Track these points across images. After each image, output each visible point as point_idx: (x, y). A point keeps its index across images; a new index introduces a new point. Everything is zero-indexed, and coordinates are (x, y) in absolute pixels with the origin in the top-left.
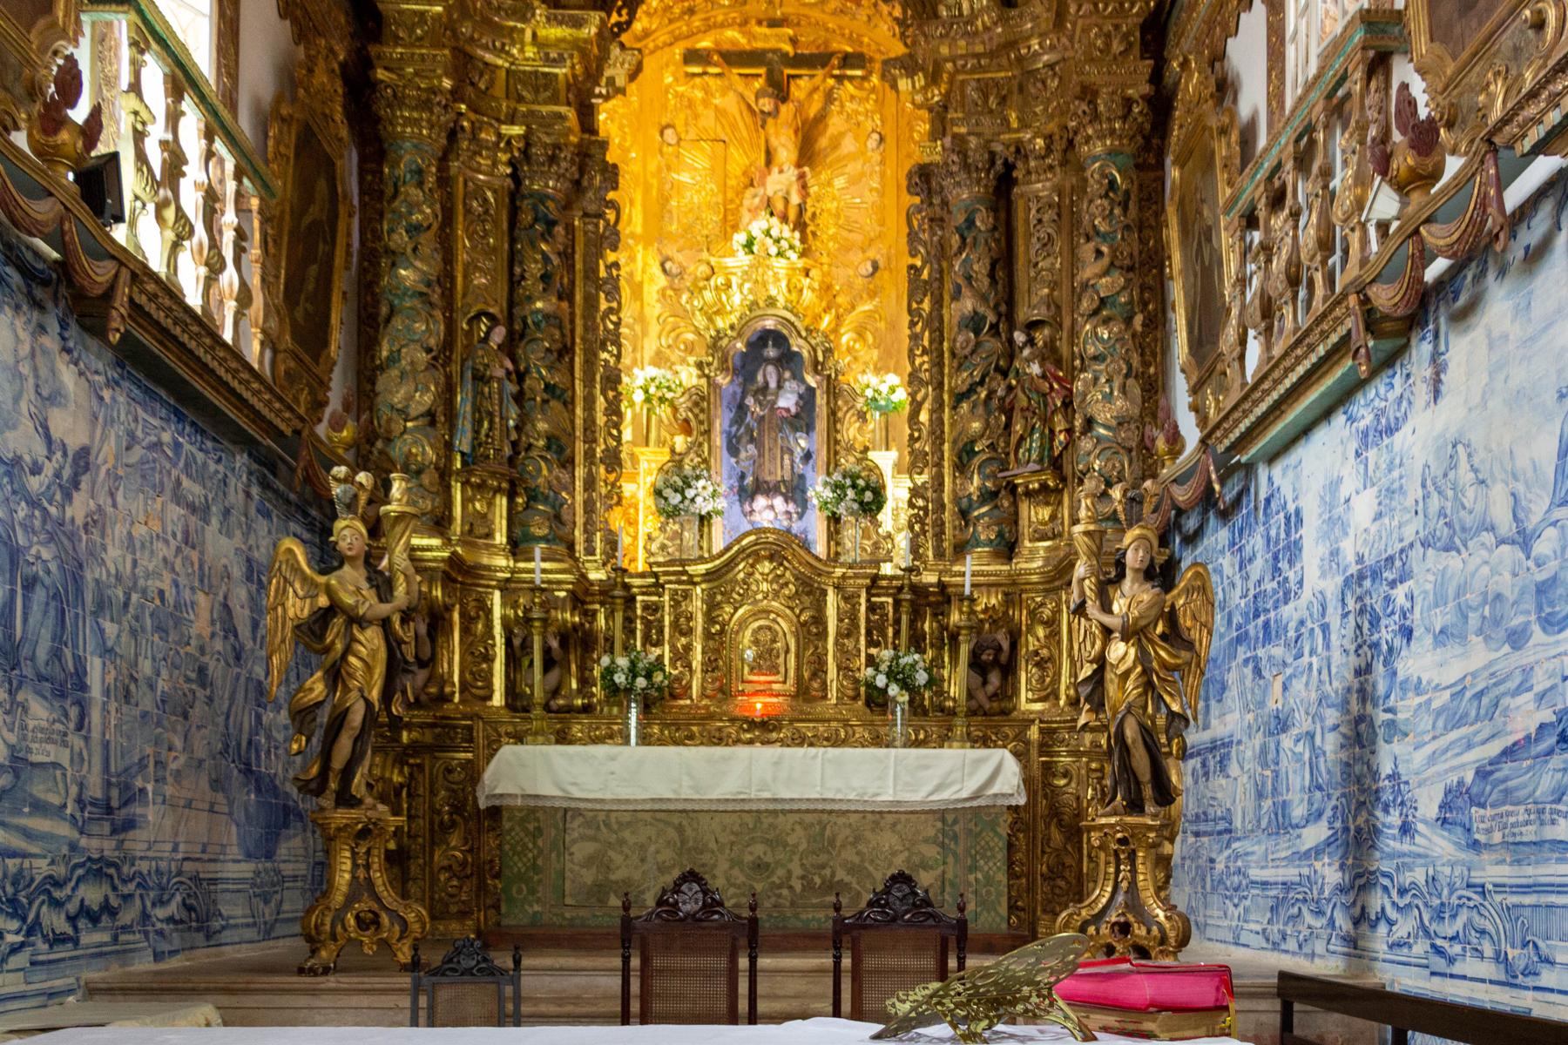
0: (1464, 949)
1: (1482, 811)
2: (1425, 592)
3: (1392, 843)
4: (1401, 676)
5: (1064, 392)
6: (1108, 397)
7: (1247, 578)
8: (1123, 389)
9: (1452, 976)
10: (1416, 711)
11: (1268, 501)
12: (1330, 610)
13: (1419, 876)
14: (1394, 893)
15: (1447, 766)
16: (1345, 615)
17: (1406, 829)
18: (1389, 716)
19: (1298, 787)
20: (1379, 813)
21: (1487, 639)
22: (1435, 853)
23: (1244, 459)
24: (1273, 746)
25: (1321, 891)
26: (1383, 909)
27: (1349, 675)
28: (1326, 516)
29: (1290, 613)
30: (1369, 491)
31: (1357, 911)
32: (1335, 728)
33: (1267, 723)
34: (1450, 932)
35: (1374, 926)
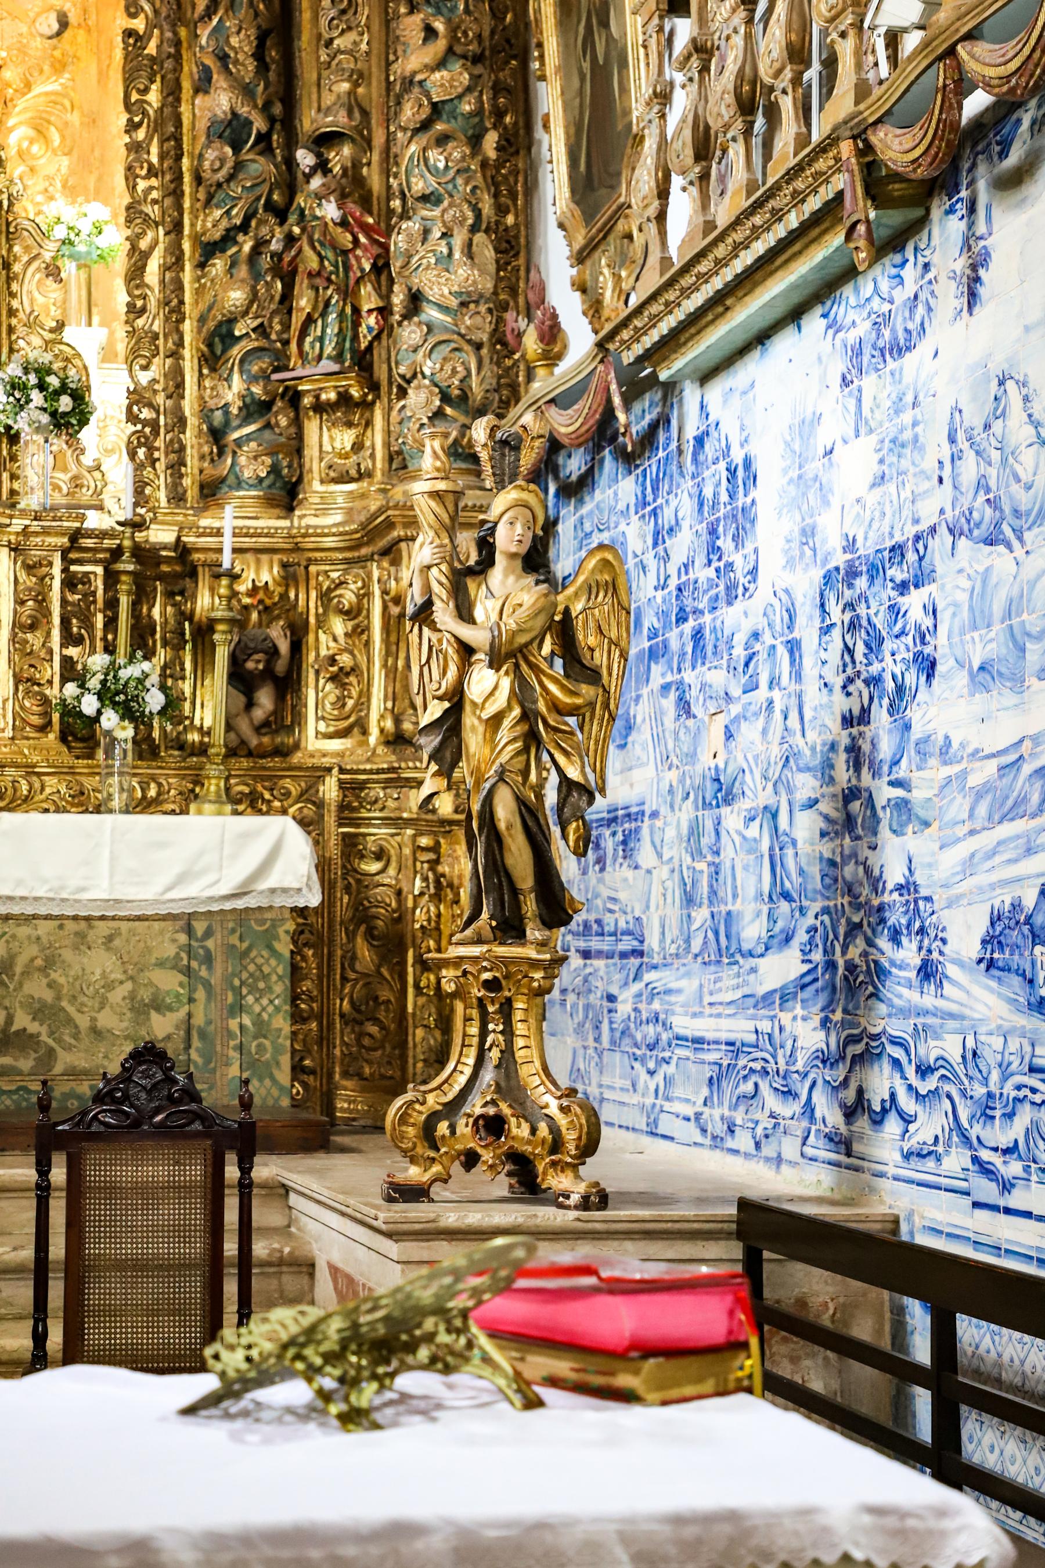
2: (956, 605)
5: (376, 250)
7: (666, 558)
11: (700, 441)
12: (801, 620)
16: (826, 630)
23: (663, 375)
27: (834, 724)
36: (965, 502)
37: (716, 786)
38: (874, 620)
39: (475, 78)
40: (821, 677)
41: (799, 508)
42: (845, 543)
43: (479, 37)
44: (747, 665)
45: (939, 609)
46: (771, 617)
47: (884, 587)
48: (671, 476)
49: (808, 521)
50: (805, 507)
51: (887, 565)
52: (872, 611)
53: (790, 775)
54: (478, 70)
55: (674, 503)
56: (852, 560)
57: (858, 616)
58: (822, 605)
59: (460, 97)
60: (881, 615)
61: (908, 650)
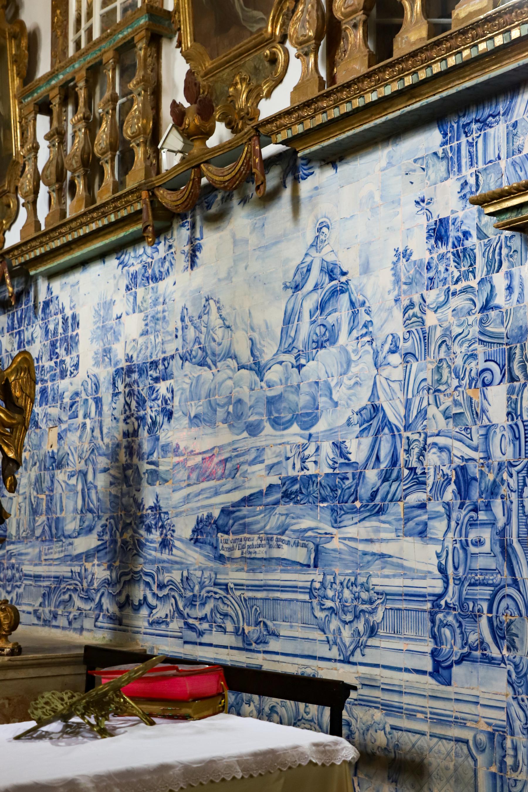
0: (211, 626)
1: (226, 536)
2: (183, 389)
3: (153, 553)
4: (163, 441)
9: (201, 644)
10: (174, 466)
11: (47, 304)
12: (102, 389)
13: (176, 576)
14: (155, 588)
15: (199, 504)
16: (115, 395)
17: (165, 544)
18: (153, 467)
19: (71, 508)
20: (142, 532)
21: (231, 426)
22: (190, 560)
23: (32, 273)
24: (48, 478)
25: (91, 583)
26: (145, 598)
27: (119, 436)
28: (101, 325)
31: (122, 598)
32: (105, 470)
33: (43, 461)
34: (200, 614)
35: (137, 609)
37: (52, 460)
38: (141, 392)
40: (112, 415)
41: (103, 340)
42: (126, 358)
44: (71, 406)
45: (175, 390)
46: (86, 386)
47: (147, 378)
48: (30, 318)
49: (107, 346)
50: (105, 340)
51: (149, 369)
52: (140, 389)
53: (94, 457)
55: (31, 330)
56: (131, 365)
57: (133, 390)
58: (114, 384)
60: (145, 390)
61: (159, 406)
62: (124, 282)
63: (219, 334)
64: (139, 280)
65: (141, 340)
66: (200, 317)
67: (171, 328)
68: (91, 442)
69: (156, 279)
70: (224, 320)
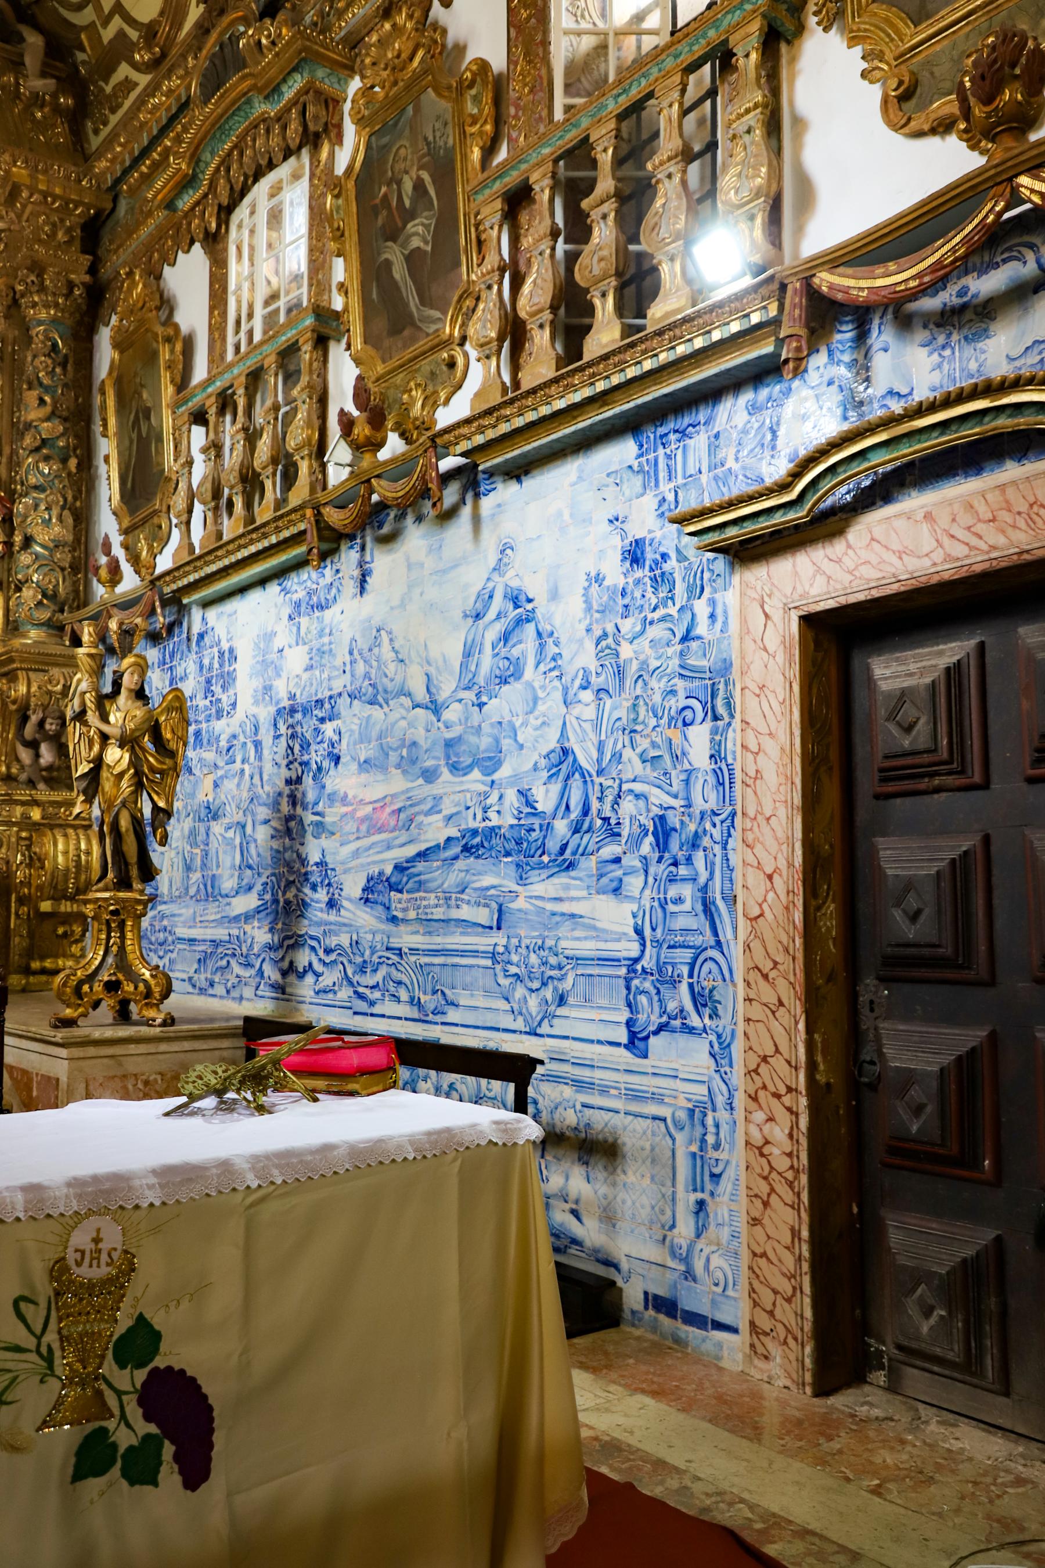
0: (383, 995)
1: (399, 895)
2: (352, 731)
3: (319, 914)
4: (329, 789)
6: (47, 523)
8: (60, 518)
9: (372, 1015)
11: (201, 636)
12: (262, 731)
13: (344, 940)
14: (321, 952)
15: (369, 860)
16: (277, 737)
17: (332, 904)
18: (318, 818)
19: (228, 864)
20: (307, 890)
21: (405, 772)
22: (360, 922)
24: (202, 830)
26: (310, 964)
27: (281, 784)
29: (223, 727)
30: (300, 647)
31: (285, 964)
32: (266, 822)
34: (371, 983)
35: (301, 976)
36: (358, 684)
39: (66, 429)
43: (68, 408)
54: (68, 425)
55: (184, 665)
59: (58, 438)
62: (287, 611)
63: (391, 668)
64: (303, 609)
65: (305, 676)
66: (370, 650)
67: (338, 662)
68: (250, 790)
69: (321, 607)
70: (397, 652)
